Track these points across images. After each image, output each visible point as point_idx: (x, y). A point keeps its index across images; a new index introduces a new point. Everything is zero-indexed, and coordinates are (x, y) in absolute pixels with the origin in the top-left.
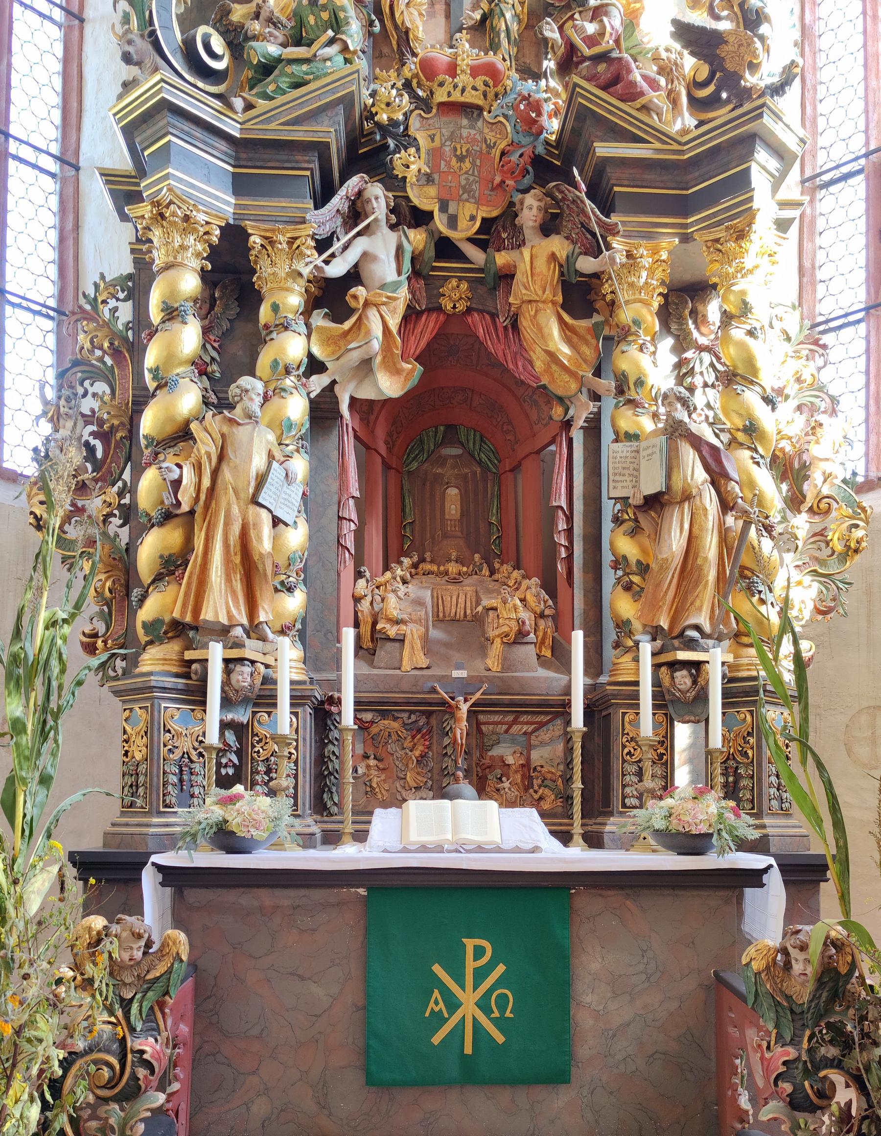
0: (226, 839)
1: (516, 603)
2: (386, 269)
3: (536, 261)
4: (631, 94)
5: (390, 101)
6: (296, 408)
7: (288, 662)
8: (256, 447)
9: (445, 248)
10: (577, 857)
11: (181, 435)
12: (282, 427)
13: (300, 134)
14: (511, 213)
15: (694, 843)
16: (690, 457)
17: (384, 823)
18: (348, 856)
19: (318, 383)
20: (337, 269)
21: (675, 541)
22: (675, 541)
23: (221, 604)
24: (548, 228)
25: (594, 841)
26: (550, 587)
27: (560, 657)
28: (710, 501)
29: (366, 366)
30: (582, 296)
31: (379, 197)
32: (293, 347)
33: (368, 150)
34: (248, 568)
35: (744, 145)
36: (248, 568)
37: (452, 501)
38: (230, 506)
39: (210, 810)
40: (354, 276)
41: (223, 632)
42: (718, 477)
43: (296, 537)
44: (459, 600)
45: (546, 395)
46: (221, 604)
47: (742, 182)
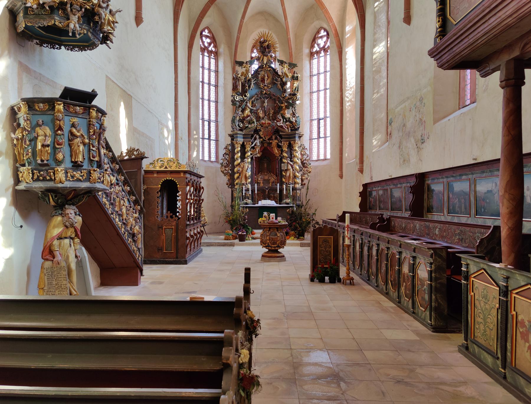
0: (246, 204)
1: (273, 179)
2: (258, 144)
3: (274, 142)
4: (284, 129)
5: (259, 127)
6: (250, 160)
7: (249, 186)
8: (246, 165)
9: (264, 140)
10: (278, 205)
11: (239, 164)
12: (248, 162)
13: (250, 133)
14: (272, 137)
15: (288, 204)
16: (289, 165)
17: (260, 202)
18: (256, 205)
19: (251, 156)
20: (253, 145)
21: (288, 174)
22: (288, 174)
23: (244, 181)
24: (275, 139)
25: (280, 204)
26: (276, 176)
27: (277, 185)
28: (292, 170)
29: (256, 154)
30: (279, 147)
31: (258, 137)
32: (249, 154)
33: (256, 131)
34: (246, 178)
35: (295, 134)
36: (246, 178)
37: (265, 165)
38: (244, 171)
39: (245, 201)
40: (255, 145)
41: (243, 184)
42: (292, 167)
43: (250, 173)
44: (266, 178)
45: (276, 157)
46: (244, 181)
47: (295, 137)
